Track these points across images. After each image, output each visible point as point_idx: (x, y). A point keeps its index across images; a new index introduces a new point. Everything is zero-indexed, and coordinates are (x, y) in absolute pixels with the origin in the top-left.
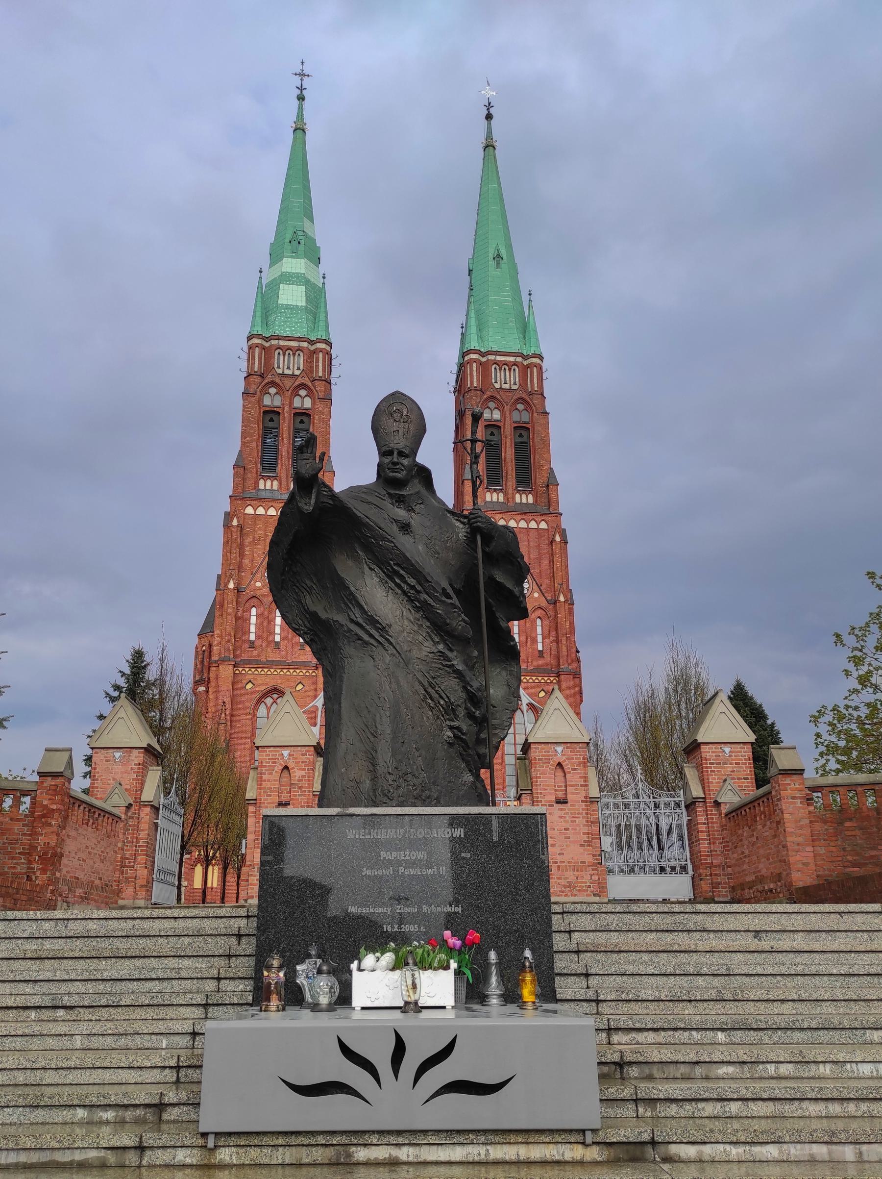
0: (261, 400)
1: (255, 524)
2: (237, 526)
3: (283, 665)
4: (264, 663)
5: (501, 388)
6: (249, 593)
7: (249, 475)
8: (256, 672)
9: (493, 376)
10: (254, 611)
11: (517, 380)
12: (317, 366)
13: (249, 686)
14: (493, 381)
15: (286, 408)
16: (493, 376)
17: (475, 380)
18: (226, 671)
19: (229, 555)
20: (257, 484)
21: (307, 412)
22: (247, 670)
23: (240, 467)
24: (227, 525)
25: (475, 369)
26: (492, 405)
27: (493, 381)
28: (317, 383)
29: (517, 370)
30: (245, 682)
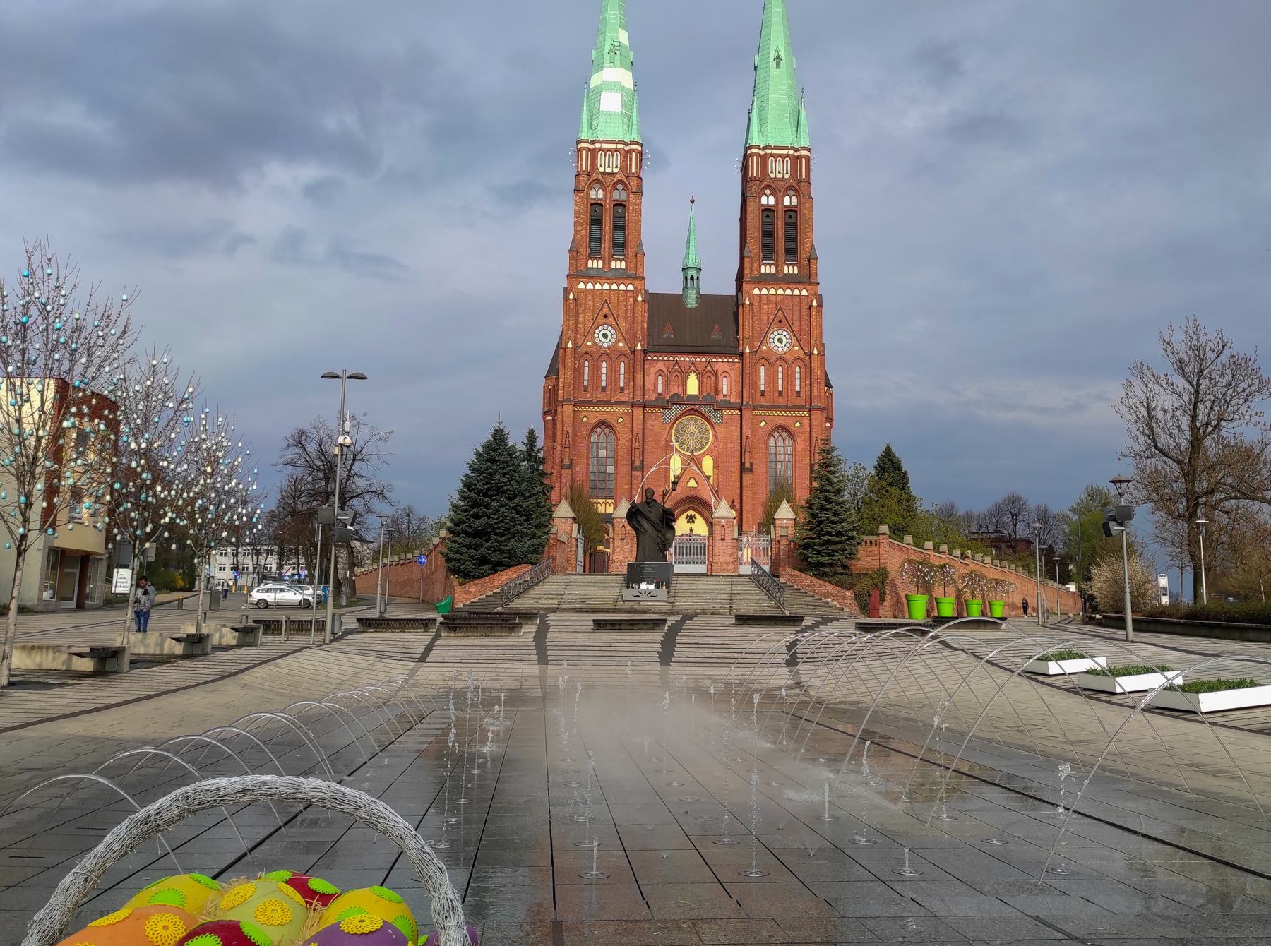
0: (588, 195)
1: (586, 296)
2: (573, 299)
3: (608, 404)
4: (595, 403)
5: (775, 178)
6: (583, 350)
10: (586, 363)
12: (631, 165)
13: (585, 419)
14: (770, 171)
15: (608, 201)
16: (770, 168)
18: (568, 409)
19: (567, 321)
20: (587, 264)
21: (624, 203)
22: (583, 407)
23: (574, 251)
24: (566, 299)
26: (768, 192)
27: (770, 171)
28: (631, 179)
30: (581, 417)
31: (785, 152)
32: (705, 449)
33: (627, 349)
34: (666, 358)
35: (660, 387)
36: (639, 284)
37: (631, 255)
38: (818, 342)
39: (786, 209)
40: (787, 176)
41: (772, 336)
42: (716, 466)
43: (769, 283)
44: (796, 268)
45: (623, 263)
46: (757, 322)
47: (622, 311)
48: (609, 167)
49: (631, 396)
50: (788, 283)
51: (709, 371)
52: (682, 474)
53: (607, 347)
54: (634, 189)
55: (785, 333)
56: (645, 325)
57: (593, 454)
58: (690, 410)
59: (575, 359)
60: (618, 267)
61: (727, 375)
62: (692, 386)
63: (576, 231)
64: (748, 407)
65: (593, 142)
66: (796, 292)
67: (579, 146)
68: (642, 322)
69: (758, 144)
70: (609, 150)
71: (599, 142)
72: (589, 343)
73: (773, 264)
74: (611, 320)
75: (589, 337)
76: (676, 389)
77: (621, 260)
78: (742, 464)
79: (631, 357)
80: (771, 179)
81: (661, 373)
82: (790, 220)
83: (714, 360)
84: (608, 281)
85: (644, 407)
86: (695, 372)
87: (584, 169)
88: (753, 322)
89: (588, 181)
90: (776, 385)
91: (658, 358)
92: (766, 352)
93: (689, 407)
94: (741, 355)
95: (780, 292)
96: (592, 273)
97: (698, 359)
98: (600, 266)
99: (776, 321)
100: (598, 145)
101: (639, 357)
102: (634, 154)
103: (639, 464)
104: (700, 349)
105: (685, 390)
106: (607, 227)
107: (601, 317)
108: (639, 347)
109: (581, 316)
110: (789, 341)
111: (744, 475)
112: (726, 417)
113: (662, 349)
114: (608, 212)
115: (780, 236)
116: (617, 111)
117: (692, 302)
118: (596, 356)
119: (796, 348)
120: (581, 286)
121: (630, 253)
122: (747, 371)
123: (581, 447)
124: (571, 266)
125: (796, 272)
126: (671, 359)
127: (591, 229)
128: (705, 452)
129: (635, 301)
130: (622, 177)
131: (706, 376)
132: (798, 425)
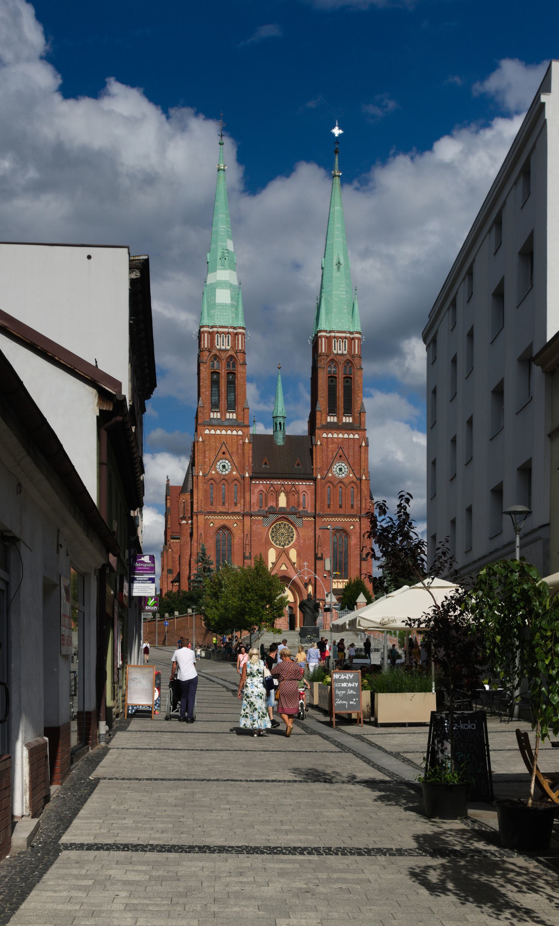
3: (227, 514)
4: (218, 513)
5: (337, 354)
6: (209, 477)
13: (212, 525)
15: (223, 371)
20: (210, 415)
28: (239, 354)
29: (347, 341)
31: (344, 335)
33: (239, 476)
34: (265, 482)
36: (245, 429)
38: (365, 471)
40: (345, 352)
41: (335, 467)
42: (298, 555)
44: (351, 418)
45: (235, 414)
47: (234, 450)
48: (223, 345)
49: (242, 508)
52: (277, 561)
53: (226, 475)
54: (241, 362)
55: (343, 465)
56: (251, 459)
58: (281, 518)
60: (231, 418)
61: (304, 493)
62: (282, 502)
66: (351, 436)
67: (202, 330)
68: (249, 457)
69: (325, 329)
70: (223, 333)
71: (216, 327)
72: (213, 472)
73: (335, 416)
74: (227, 456)
75: (213, 467)
76: (271, 504)
78: (316, 555)
79: (242, 481)
80: (335, 354)
82: (347, 384)
83: (297, 483)
85: (251, 517)
86: (284, 492)
87: (206, 347)
88: (322, 457)
89: (209, 355)
92: (331, 477)
93: (280, 516)
94: (315, 480)
95: (341, 436)
96: (214, 422)
97: (286, 483)
98: (219, 417)
99: (338, 456)
100: (215, 329)
101: (247, 481)
102: (240, 336)
104: (287, 476)
105: (277, 504)
106: (223, 388)
107: (221, 454)
108: (247, 475)
110: (347, 470)
111: (317, 561)
112: (305, 522)
113: (262, 475)
114: (223, 378)
115: (340, 396)
119: (351, 475)
120: (207, 432)
121: (239, 408)
122: (319, 492)
125: (351, 421)
126: (268, 482)
127: (211, 390)
128: (291, 547)
129: (244, 443)
132: (352, 527)
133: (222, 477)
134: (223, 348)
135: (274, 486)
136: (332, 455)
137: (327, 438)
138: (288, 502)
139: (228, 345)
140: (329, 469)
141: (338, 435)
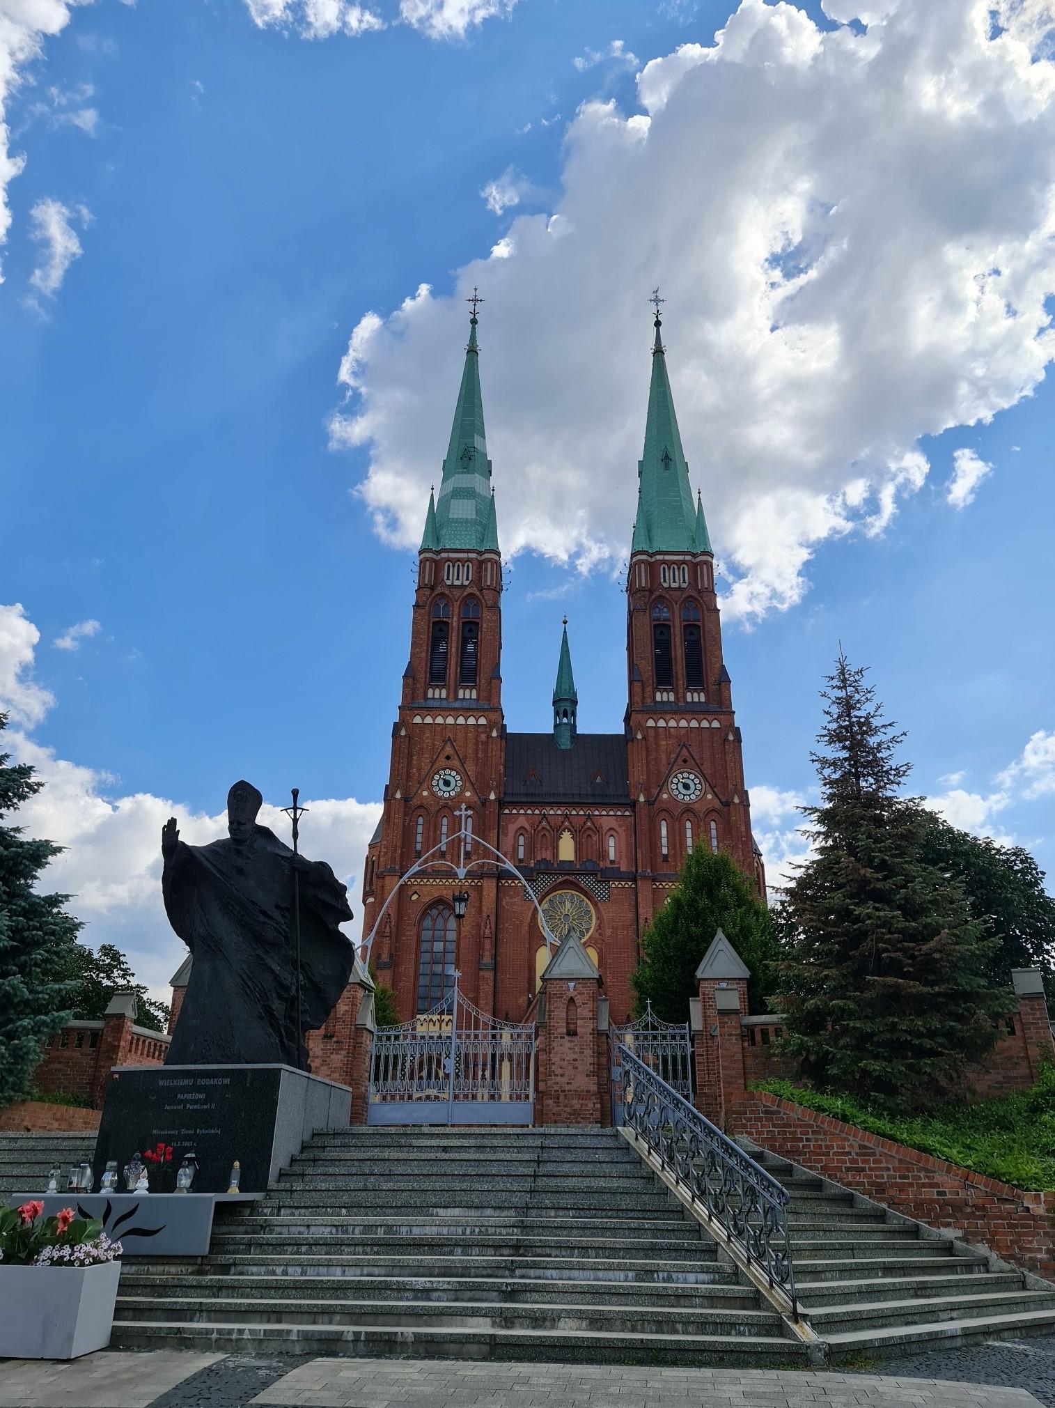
2: (405, 736)
4: (430, 874)
6: (416, 802)
7: (418, 686)
8: (422, 883)
9: (662, 576)
10: (421, 820)
11: (687, 578)
13: (415, 897)
15: (455, 618)
17: (643, 581)
20: (426, 693)
23: (409, 675)
25: (643, 570)
27: (662, 580)
30: (410, 893)
31: (680, 558)
32: (586, 938)
34: (529, 812)
35: (521, 850)
36: (493, 716)
37: (483, 681)
39: (686, 623)
40: (684, 585)
43: (666, 712)
44: (702, 695)
46: (653, 763)
47: (471, 750)
50: (693, 712)
51: (589, 828)
53: (450, 798)
54: (490, 603)
55: (692, 777)
57: (425, 946)
58: (564, 882)
59: (406, 814)
61: (612, 832)
62: (567, 849)
63: (413, 655)
64: (645, 878)
65: (438, 553)
66: (705, 724)
70: (459, 560)
73: (671, 690)
74: (456, 763)
77: (471, 688)
81: (522, 831)
82: (691, 638)
83: (597, 813)
84: (452, 713)
86: (569, 830)
89: (430, 595)
90: (683, 846)
91: (518, 811)
94: (633, 805)
95: (683, 723)
96: (431, 704)
97: (574, 812)
99: (680, 761)
100: (444, 555)
102: (489, 564)
103: (490, 961)
107: (442, 759)
108: (492, 797)
109: (415, 758)
116: (469, 517)
117: (565, 743)
118: (433, 810)
119: (709, 796)
121: (482, 679)
123: (411, 932)
124: (404, 696)
125: (703, 699)
126: (537, 812)
129: (489, 737)
130: (475, 591)
131: (585, 835)
133: (441, 803)
134: (457, 583)
135: (549, 818)
136: (668, 758)
137: (656, 728)
138: (578, 850)
139: (467, 579)
140: (662, 786)
141: (678, 723)
